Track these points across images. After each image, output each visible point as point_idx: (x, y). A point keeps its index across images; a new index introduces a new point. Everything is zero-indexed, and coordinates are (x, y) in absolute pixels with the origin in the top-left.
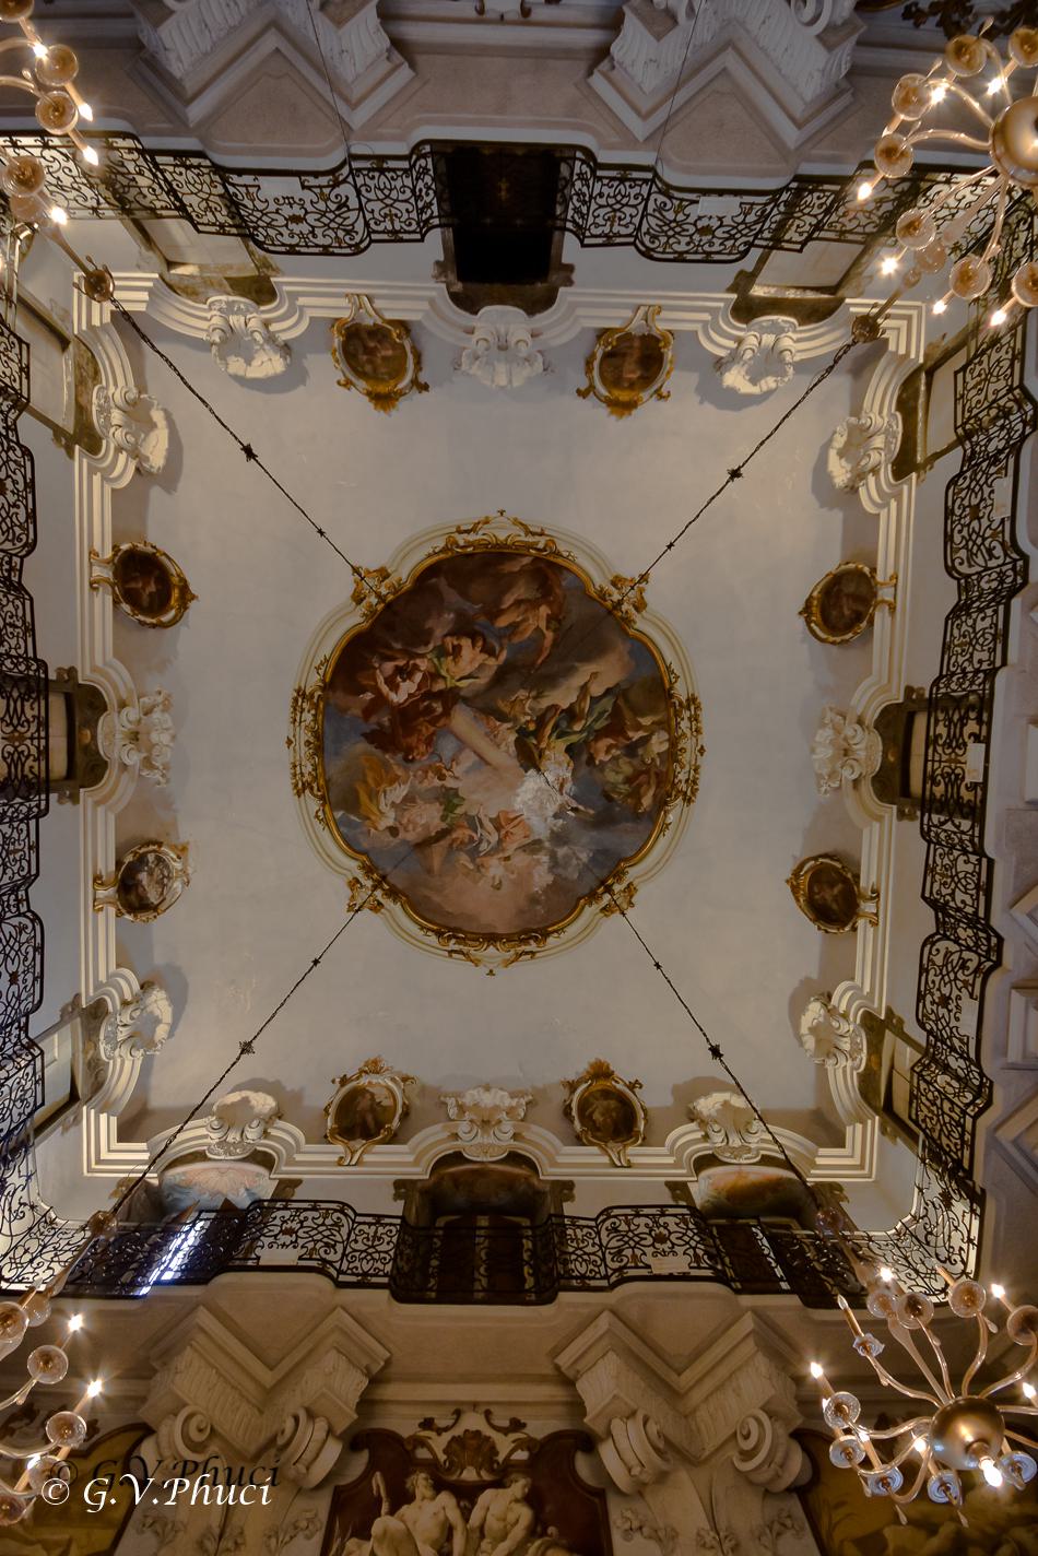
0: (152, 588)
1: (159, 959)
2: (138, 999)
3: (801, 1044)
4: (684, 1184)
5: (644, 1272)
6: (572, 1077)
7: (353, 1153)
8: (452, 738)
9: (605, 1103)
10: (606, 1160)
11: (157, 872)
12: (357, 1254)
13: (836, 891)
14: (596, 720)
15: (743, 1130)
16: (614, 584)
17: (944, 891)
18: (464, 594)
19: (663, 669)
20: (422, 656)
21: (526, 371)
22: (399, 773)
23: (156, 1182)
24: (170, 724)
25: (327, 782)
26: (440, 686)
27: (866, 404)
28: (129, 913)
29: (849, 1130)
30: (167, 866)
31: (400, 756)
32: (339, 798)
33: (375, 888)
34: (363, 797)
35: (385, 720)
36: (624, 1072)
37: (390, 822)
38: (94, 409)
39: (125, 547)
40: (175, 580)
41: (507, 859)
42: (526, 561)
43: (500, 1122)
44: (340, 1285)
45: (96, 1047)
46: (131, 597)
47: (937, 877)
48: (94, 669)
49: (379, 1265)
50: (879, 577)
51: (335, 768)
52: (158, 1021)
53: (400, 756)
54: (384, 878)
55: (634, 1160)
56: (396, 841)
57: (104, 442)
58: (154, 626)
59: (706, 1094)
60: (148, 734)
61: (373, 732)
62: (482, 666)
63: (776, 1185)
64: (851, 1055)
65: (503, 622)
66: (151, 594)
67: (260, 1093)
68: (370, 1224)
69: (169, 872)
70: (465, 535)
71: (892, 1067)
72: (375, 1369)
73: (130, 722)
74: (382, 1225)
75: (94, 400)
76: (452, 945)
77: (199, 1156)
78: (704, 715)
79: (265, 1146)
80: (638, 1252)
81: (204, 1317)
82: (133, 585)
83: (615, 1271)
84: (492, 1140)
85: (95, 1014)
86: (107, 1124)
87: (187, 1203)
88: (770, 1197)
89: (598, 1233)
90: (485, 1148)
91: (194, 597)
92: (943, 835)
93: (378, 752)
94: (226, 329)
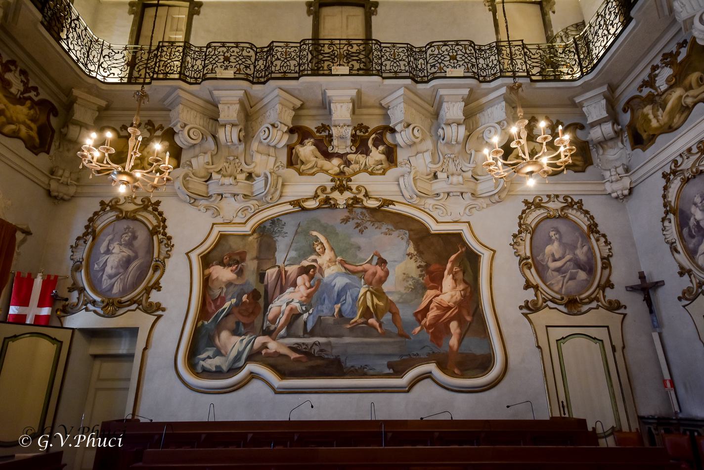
17: (279, 54)
47: (284, 49)
92: (305, 53)
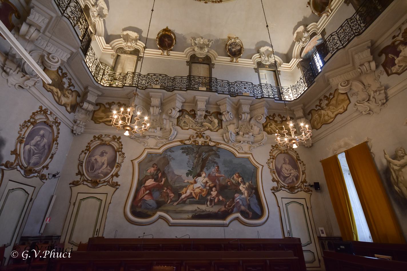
0: (166, 39)
1: (253, 47)
2: (261, 55)
11: (233, 46)
12: (343, 38)
23: (302, 59)
24: (199, 39)
28: (240, 55)
30: (232, 43)
38: (129, 50)
39: (159, 47)
40: (164, 33)
44: (344, 47)
45: (266, 65)
46: (170, 45)
48: (186, 57)
49: (350, 34)
52: (268, 50)
57: (136, 48)
58: (175, 40)
60: (200, 44)
66: (168, 40)
68: (341, 30)
69: (234, 42)
72: (370, 45)
73: (198, 49)
74: (343, 27)
75: (128, 49)
77: (303, 49)
79: (310, 33)
81: (326, 74)
82: (167, 45)
85: (260, 65)
86: (285, 65)
87: (311, 54)
91: (167, 28)
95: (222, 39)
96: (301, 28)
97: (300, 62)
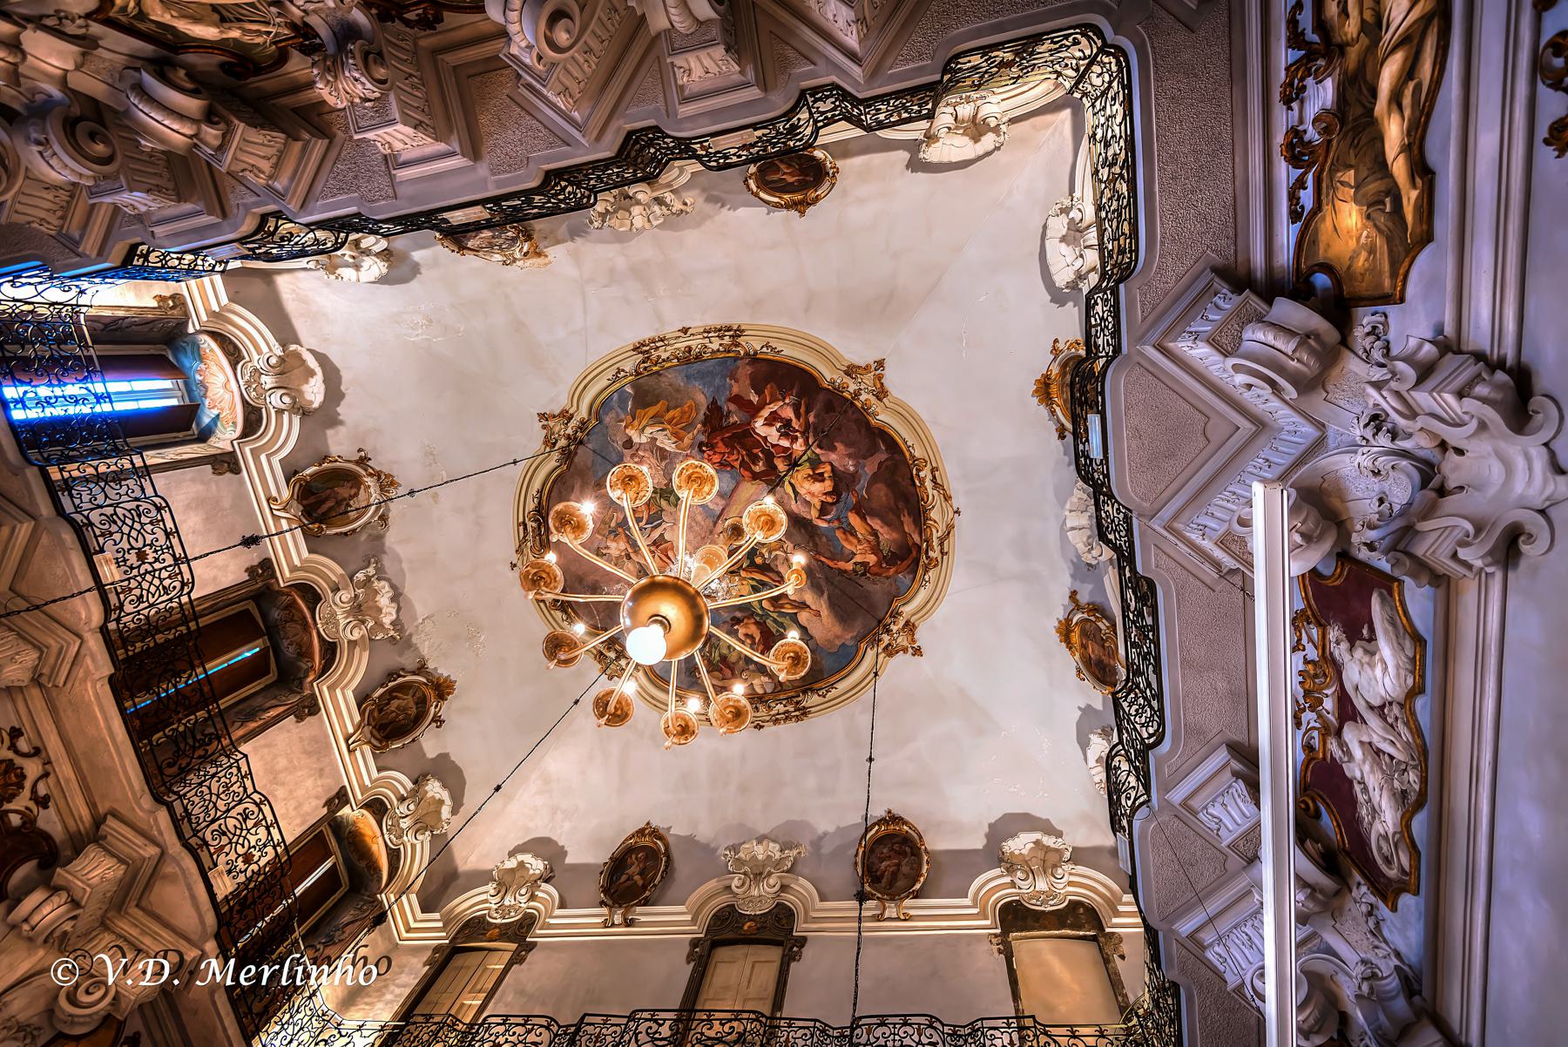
3: (512, 854)
4: (347, 802)
5: (207, 863)
6: (431, 665)
7: (284, 509)
8: (732, 486)
9: (412, 704)
10: (351, 730)
13: (637, 878)
14: (775, 621)
15: (421, 826)
16: (907, 623)
18: (875, 478)
19: (832, 680)
20: (808, 447)
21: (1081, 547)
22: (686, 441)
23: (191, 330)
25: (657, 372)
26: (781, 466)
27: (1080, 869)
29: (437, 916)
31: (703, 438)
32: (647, 386)
33: (568, 437)
34: (652, 411)
35: (734, 419)
36: (447, 709)
37: (636, 439)
41: (629, 557)
42: (916, 538)
43: (363, 622)
50: (907, 902)
51: (675, 378)
53: (703, 438)
54: (581, 442)
55: (358, 753)
56: (619, 446)
59: (444, 786)
61: (720, 408)
62: (808, 503)
63: (374, 867)
64: (501, 908)
65: (854, 520)
67: (323, 387)
70: (930, 477)
71: (490, 950)
76: (531, 525)
78: (791, 725)
80: (227, 849)
83: (203, 840)
84: (342, 623)
88: (363, 864)
89: (240, 802)
90: (335, 617)
91: (802, 213)
93: (701, 416)
94: (1084, 224)
95: (563, 241)
96: (314, 392)
97: (187, 316)
